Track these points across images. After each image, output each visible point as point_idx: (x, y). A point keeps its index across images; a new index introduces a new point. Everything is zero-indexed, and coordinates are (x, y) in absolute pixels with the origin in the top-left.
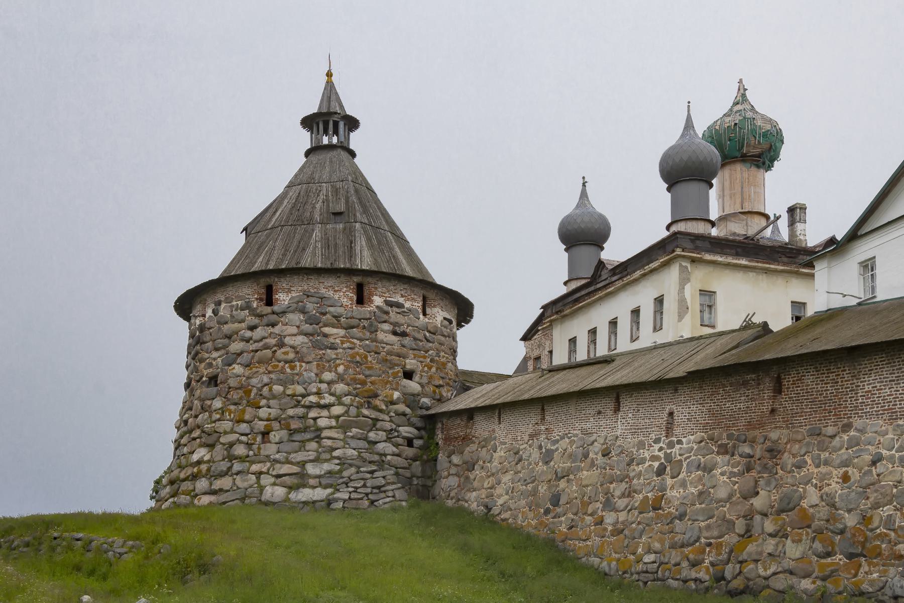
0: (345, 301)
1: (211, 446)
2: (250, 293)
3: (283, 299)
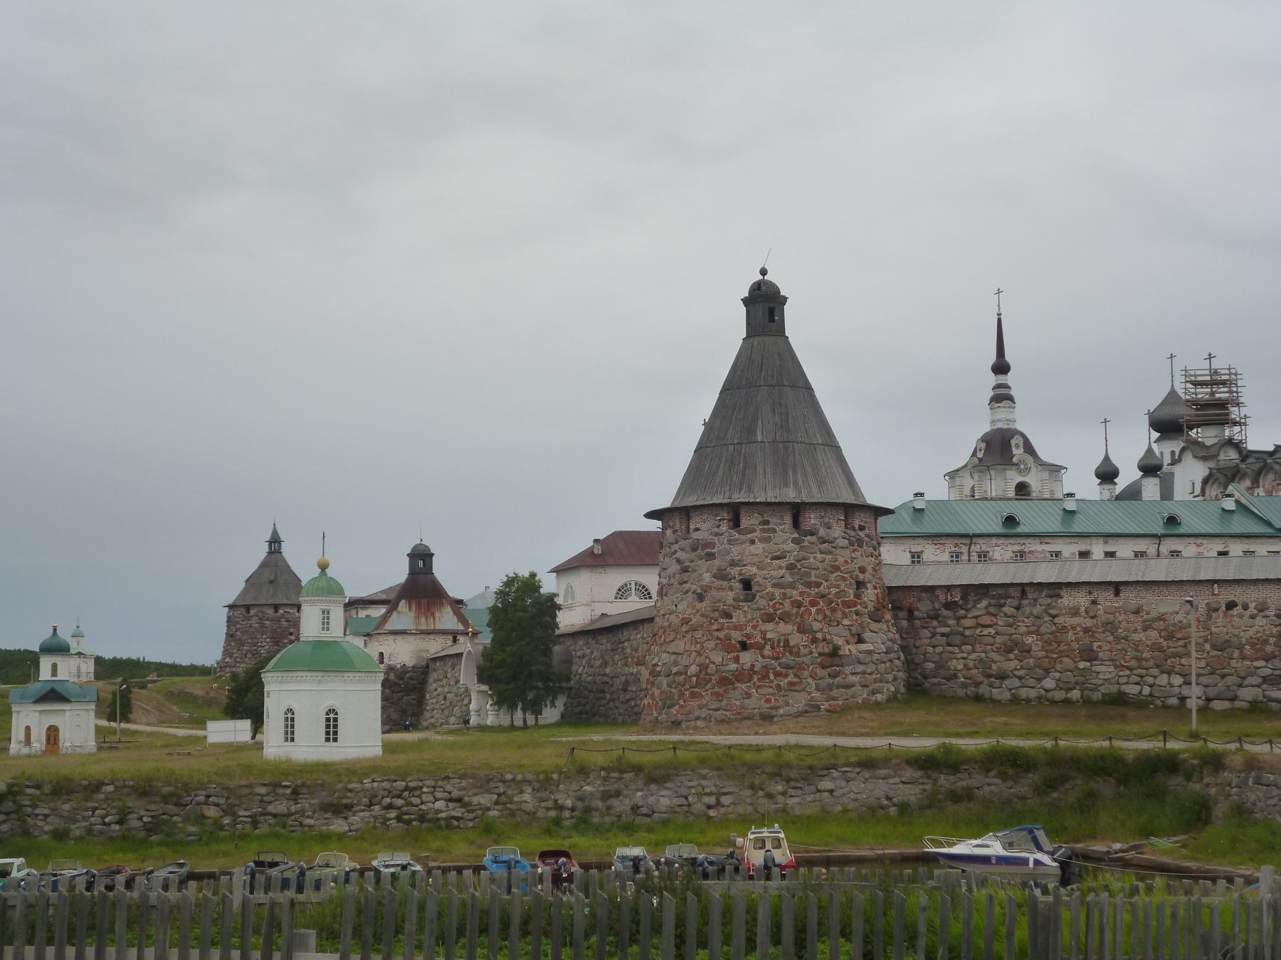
0: (271, 613)
1: (231, 657)
2: (243, 610)
3: (252, 612)
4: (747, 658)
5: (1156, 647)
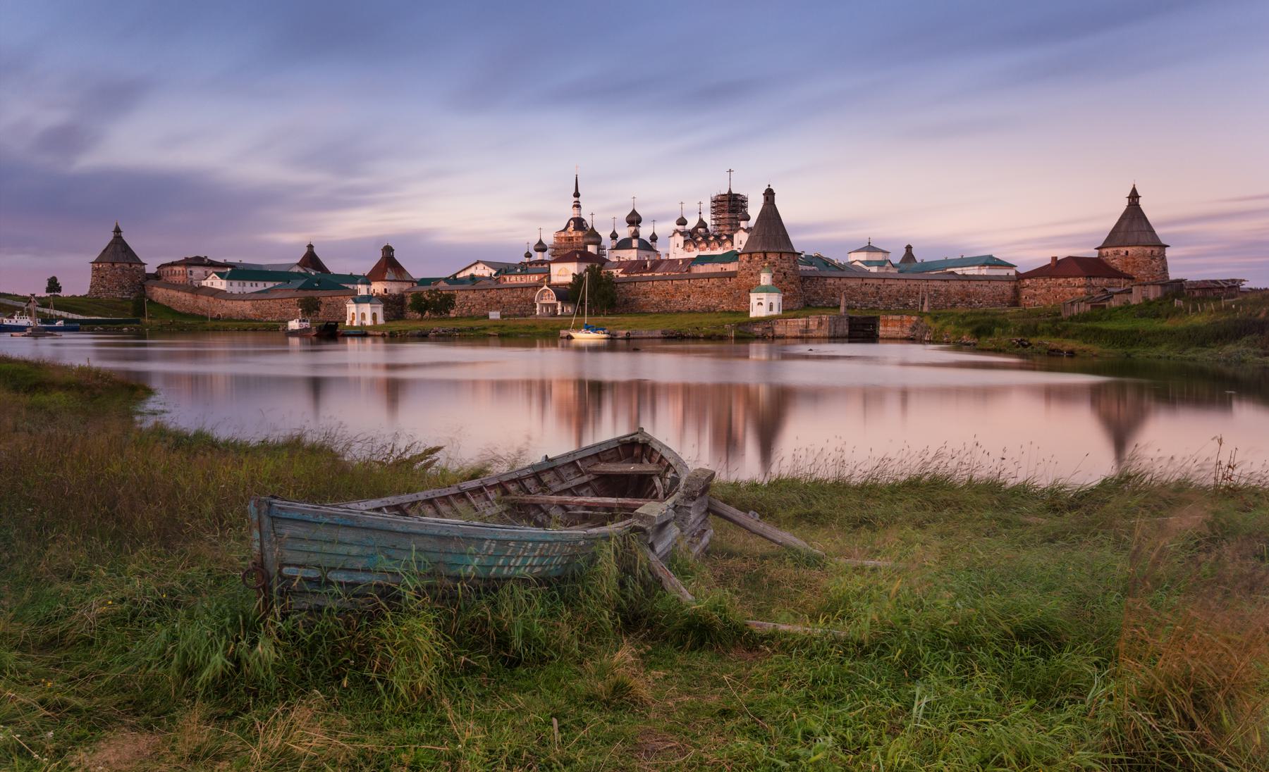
3: (117, 266)
4: (787, 293)
5: (849, 294)
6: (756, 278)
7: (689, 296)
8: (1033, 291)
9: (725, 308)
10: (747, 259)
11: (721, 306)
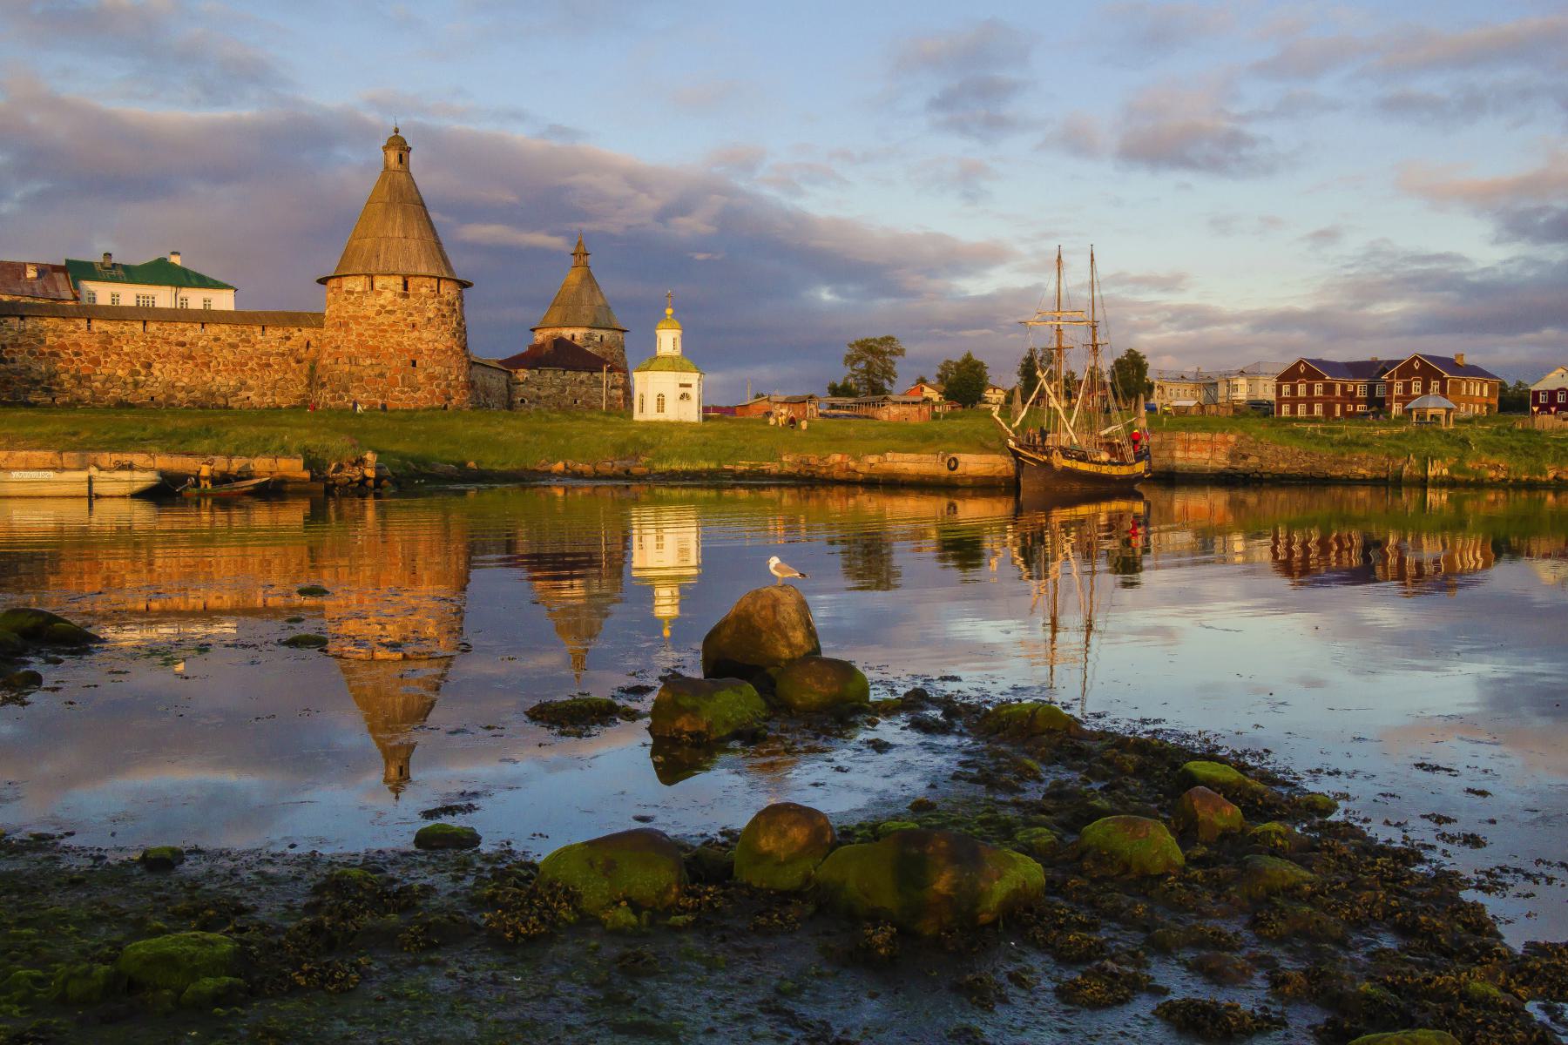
6: (426, 335)
7: (149, 366)
8: (534, 390)
9: (255, 399)
10: (400, 289)
11: (244, 394)
